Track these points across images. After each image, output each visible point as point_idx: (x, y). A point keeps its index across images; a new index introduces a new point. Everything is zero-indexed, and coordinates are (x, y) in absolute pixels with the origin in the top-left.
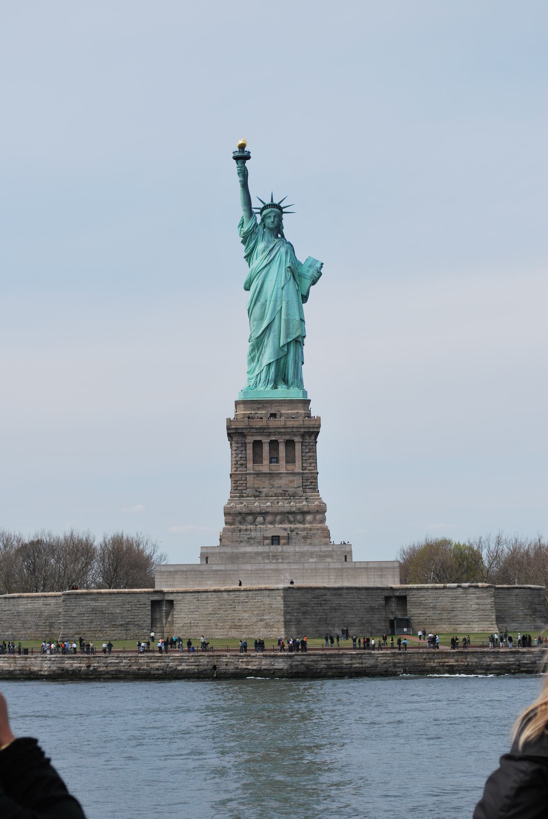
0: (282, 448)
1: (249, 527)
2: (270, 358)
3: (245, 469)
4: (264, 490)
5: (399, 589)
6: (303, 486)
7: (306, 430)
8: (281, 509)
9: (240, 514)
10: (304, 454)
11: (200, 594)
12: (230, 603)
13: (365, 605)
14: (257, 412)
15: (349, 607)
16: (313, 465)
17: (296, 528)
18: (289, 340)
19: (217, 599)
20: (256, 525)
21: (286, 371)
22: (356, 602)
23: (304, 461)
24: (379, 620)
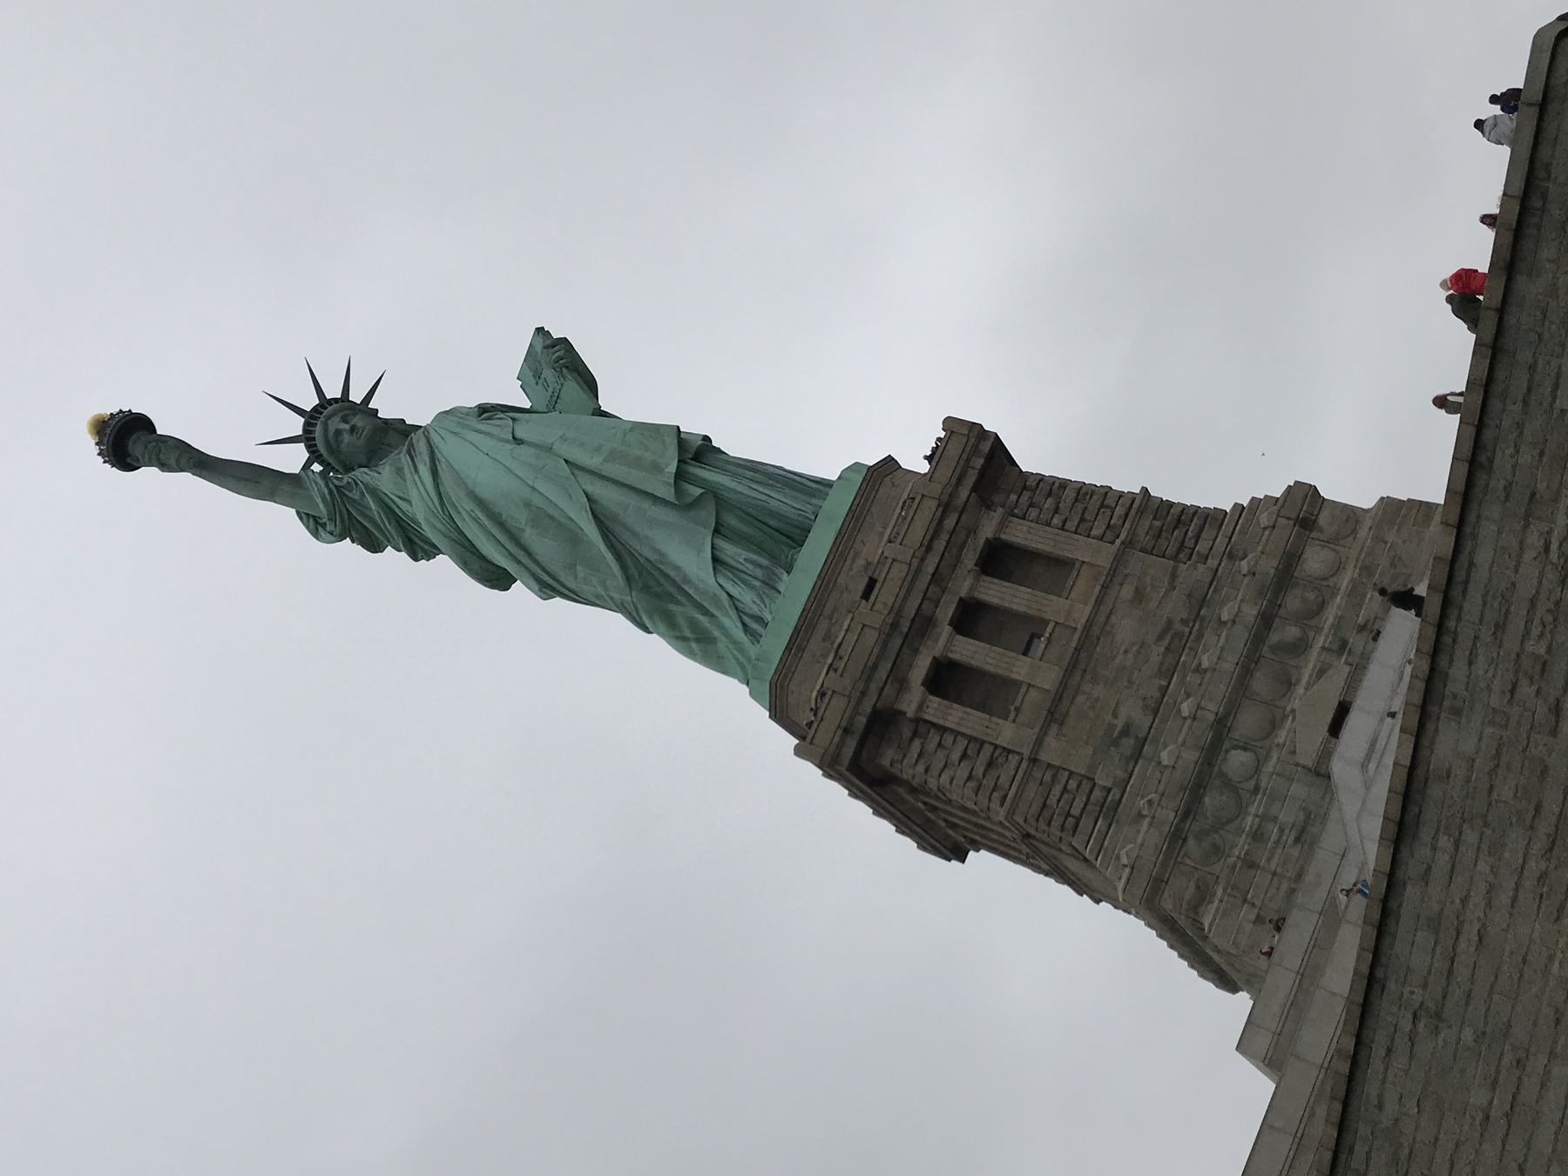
0: (995, 592)
1: (1250, 819)
2: (699, 551)
3: (1014, 759)
4: (1123, 712)
6: (1175, 558)
8: (1228, 665)
9: (1177, 837)
11: (1392, 986)
12: (1542, 710)
14: (836, 645)
16: (1110, 501)
18: (673, 468)
19: (1470, 837)
21: (773, 523)
23: (1083, 526)
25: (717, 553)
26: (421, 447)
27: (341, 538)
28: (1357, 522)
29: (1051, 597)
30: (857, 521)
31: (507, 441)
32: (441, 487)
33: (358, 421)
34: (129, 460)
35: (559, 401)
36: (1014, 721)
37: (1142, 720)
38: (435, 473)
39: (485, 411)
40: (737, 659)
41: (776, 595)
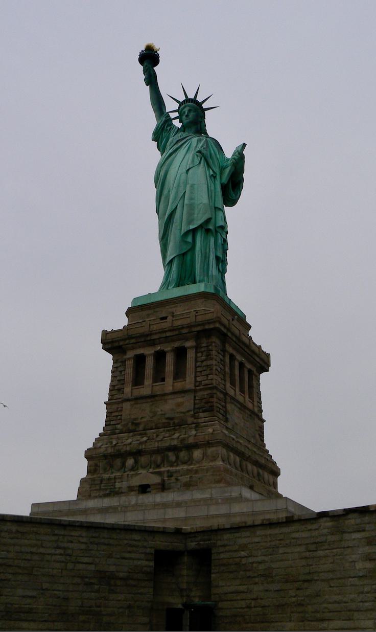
0: (170, 359)
2: (171, 255)
3: (121, 396)
5: (197, 532)
7: (199, 328)
9: (105, 456)
10: (198, 364)
13: (81, 566)
15: (19, 567)
16: (210, 377)
17: (176, 472)
18: (192, 227)
20: (125, 472)
22: (49, 557)
23: (198, 374)
24: (129, 607)
28: (215, 460)
29: (172, 378)
30: (187, 299)
36: (132, 389)
37: (141, 427)
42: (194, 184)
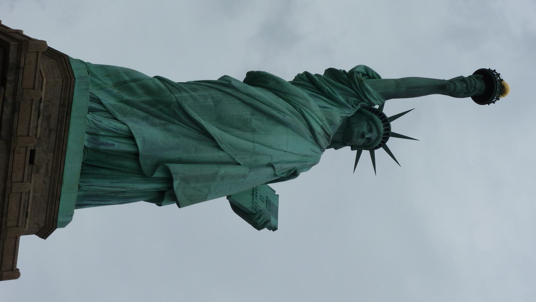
2: (144, 140)
14: (41, 116)
18: (176, 184)
21: (103, 171)
25: (132, 143)
26: (323, 141)
27: (352, 72)
31: (276, 163)
32: (306, 123)
33: (361, 141)
34: (482, 76)
35: (252, 193)
38: (312, 130)
39: (293, 174)
40: (98, 79)
41: (88, 130)
42: (245, 178)
